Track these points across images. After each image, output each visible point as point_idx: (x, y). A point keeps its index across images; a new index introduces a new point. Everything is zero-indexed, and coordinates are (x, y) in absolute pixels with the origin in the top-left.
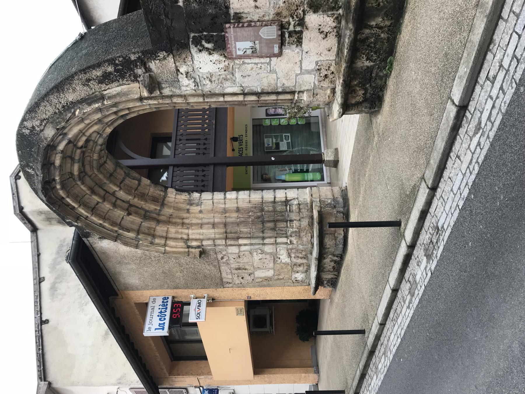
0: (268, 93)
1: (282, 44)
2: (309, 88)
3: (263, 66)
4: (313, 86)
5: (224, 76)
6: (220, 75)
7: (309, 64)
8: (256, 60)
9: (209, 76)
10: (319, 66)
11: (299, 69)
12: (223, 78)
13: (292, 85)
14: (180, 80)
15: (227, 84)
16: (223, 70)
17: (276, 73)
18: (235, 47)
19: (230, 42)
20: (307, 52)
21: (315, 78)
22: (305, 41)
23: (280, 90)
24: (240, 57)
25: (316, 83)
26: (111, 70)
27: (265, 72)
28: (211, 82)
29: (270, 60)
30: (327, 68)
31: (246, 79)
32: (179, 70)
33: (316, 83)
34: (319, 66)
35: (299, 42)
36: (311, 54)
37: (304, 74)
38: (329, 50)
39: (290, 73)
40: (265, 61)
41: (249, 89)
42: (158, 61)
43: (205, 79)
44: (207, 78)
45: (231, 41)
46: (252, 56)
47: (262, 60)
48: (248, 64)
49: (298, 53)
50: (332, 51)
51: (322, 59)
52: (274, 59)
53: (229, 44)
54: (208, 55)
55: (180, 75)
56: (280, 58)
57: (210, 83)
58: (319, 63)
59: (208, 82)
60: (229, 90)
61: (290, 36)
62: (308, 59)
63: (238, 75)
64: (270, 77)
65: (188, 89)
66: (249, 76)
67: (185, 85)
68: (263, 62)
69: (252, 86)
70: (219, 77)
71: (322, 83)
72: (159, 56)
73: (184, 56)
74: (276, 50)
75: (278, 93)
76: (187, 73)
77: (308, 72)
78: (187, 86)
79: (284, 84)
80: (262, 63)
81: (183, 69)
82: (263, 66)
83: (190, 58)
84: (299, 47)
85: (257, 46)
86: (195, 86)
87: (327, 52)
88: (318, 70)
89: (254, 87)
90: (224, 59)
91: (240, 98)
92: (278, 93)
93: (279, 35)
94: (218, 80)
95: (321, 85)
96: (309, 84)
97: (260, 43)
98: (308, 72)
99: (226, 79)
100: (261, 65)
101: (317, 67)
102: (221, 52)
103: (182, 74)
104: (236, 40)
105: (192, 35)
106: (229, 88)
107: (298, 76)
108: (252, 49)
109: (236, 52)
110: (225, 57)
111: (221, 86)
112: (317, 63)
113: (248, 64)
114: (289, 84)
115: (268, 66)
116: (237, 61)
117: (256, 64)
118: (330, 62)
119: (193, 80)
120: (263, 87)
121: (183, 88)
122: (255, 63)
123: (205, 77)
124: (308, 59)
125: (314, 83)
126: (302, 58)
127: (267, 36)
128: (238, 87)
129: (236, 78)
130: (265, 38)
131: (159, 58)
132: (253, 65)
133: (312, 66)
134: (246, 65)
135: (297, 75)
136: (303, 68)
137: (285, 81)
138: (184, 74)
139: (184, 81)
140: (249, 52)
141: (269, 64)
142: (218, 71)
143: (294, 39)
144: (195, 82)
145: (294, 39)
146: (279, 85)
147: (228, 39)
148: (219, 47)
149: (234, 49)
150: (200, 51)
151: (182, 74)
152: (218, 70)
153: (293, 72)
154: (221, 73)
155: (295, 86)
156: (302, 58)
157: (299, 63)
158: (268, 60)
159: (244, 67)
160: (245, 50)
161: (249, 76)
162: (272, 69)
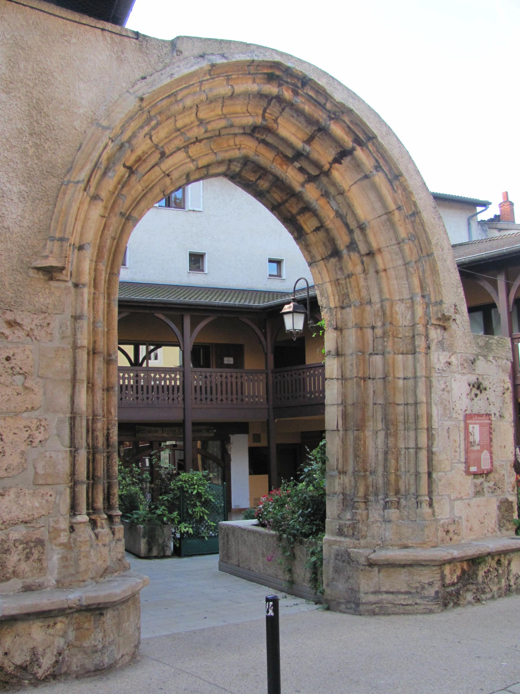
0: (430, 461)
2: (436, 514)
8: (462, 447)
9: (448, 389)
12: (446, 405)
13: (440, 490)
18: (475, 424)
20: (469, 504)
21: (446, 519)
23: (434, 475)
27: (452, 456)
29: (462, 463)
30: (455, 532)
33: (442, 522)
38: (470, 530)
44: (447, 386)
45: (480, 420)
46: (468, 442)
47: (463, 454)
52: (462, 467)
56: (464, 473)
59: (443, 386)
74: (473, 469)
75: (430, 474)
78: (439, 360)
79: (440, 480)
88: (454, 521)
89: (438, 443)
91: (424, 424)
92: (430, 474)
93: (483, 472)
100: (458, 451)
101: (456, 519)
103: (450, 357)
107: (448, 496)
109: (472, 424)
112: (460, 517)
113: (460, 437)
115: (456, 461)
116: (462, 424)
117: (459, 447)
120: (437, 454)
122: (460, 444)
125: (442, 519)
132: (458, 443)
133: (457, 513)
135: (449, 496)
137: (443, 481)
141: (459, 462)
149: (473, 422)
155: (438, 495)
158: (463, 460)
162: (454, 465)
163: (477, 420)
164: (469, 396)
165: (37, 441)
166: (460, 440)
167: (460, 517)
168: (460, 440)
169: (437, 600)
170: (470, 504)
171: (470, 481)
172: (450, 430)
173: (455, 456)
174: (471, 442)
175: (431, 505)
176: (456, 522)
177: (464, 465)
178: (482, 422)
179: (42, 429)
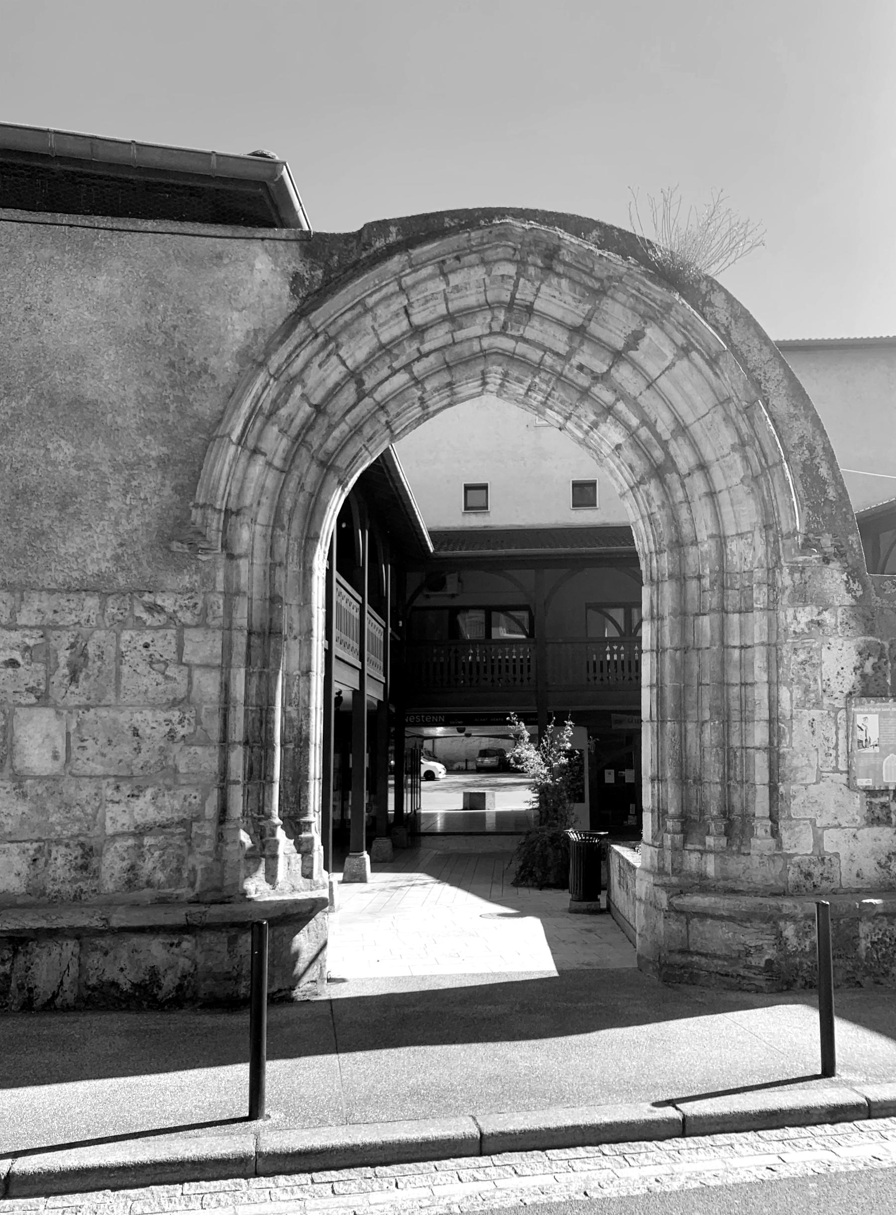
1: (871, 792)
2: (785, 846)
3: (832, 758)
4: (788, 852)
5: (813, 687)
6: (815, 680)
7: (832, 842)
9: (814, 661)
10: (830, 860)
11: (824, 824)
13: (792, 811)
14: (808, 609)
15: (798, 693)
16: (824, 687)
17: (817, 783)
18: (870, 713)
19: (878, 704)
20: (854, 836)
21: (806, 855)
22: (876, 831)
24: (850, 719)
25: (796, 859)
26: (830, 495)
27: (820, 762)
28: (802, 663)
29: (842, 772)
30: (825, 875)
31: (806, 726)
32: (826, 610)
33: (796, 859)
34: (830, 860)
35: (874, 821)
36: (851, 843)
37: (815, 833)
38: (858, 875)
39: (816, 808)
40: (840, 762)
41: (786, 731)
42: (846, 579)
43: (809, 653)
44: (811, 657)
45: (880, 707)
47: (842, 758)
48: (837, 733)
49: (854, 820)
50: (858, 879)
51: (844, 863)
53: (876, 702)
54: (853, 666)
55: (816, 610)
57: (799, 660)
58: (834, 859)
60: (784, 694)
61: (884, 806)
62: (843, 839)
63: (815, 713)
64: (809, 770)
65: (789, 620)
66: (813, 733)
67: (798, 615)
68: (840, 759)
69: (791, 738)
70: (812, 677)
71: (796, 869)
72: (854, 582)
73: (853, 624)
74: (862, 782)
76: (819, 624)
77: (818, 841)
78: (795, 618)
79: (794, 797)
80: (837, 756)
81: (827, 616)
82: (832, 758)
83: (849, 633)
84: (864, 822)
85: (870, 750)
86: (795, 632)
87: (855, 872)
88: (823, 859)
90: (846, 692)
91: (763, 713)
92: (773, 789)
93: (887, 787)
94: (806, 677)
95: (792, 868)
96: (793, 845)
97: (876, 755)
98: (818, 841)
99: (806, 691)
100: (834, 754)
102: (859, 687)
103: (819, 614)
104: (883, 715)
105: (887, 644)
106: (789, 694)
107: (811, 823)
108: (866, 740)
110: (850, 693)
111: (792, 679)
112: (837, 855)
113: (837, 733)
114: (796, 807)
115: (830, 769)
116: (842, 714)
118: (838, 878)
119: (807, 631)
120: (789, 757)
121: (790, 612)
122: (837, 745)
123: (811, 654)
124: (843, 839)
125: (796, 854)
126: (845, 827)
127: (886, 767)
128: (792, 710)
129: (809, 709)
130: (884, 763)
131: (851, 581)
132: (834, 741)
133: (828, 847)
134: (834, 730)
135: (813, 822)
136: (826, 832)
138: (819, 618)
139: (805, 615)
140: (860, 735)
141: (836, 770)
142: (824, 678)
143: (878, 812)
144: (803, 632)
145: (878, 812)
146: (793, 787)
147: (883, 702)
148: (867, 685)
149: (866, 710)
150: (860, 654)
151: (819, 614)
152: (825, 677)
153: (819, 813)
154: (819, 681)
155: (790, 818)
156: (845, 827)
157: (836, 823)
158: (843, 767)
159: (831, 724)
160: (864, 728)
161: (813, 733)
162: (824, 774)
163: (874, 707)
164: (858, 672)
165: (179, 736)
166: (837, 739)
167: (837, 855)
168: (837, 739)
169: (770, 974)
170: (858, 835)
171: (858, 801)
172: (815, 724)
173: (825, 762)
174: (861, 741)
175: (775, 833)
176: (826, 861)
177: (845, 776)
178: (884, 710)
179: (186, 721)
